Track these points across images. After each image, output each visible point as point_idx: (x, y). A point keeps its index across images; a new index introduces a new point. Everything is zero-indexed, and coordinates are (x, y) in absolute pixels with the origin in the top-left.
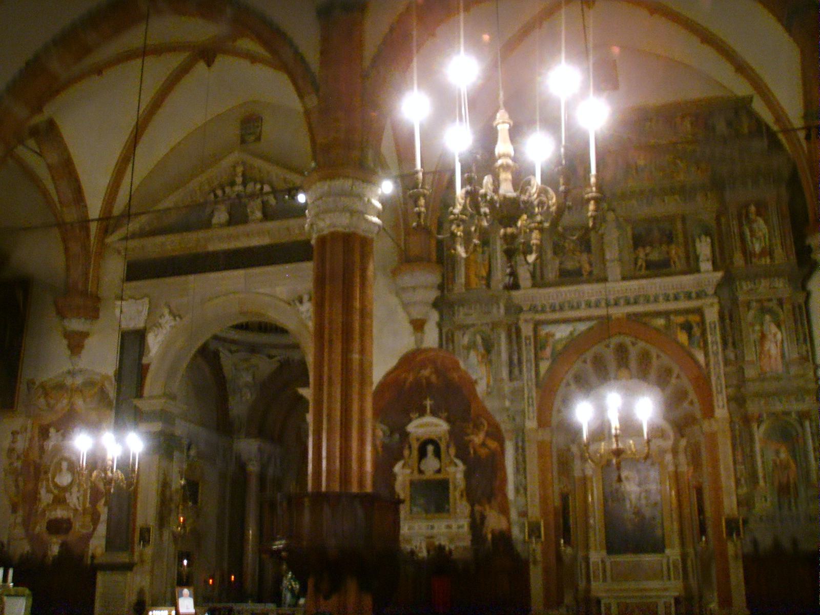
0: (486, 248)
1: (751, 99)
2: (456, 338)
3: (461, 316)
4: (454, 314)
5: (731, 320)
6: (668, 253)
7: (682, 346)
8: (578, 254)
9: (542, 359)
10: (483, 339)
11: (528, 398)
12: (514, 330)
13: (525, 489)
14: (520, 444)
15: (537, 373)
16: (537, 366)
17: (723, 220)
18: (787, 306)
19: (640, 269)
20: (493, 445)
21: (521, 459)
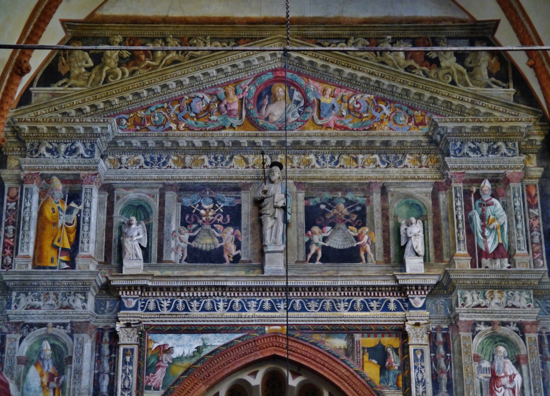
0: (73, 204)
1: (496, 24)
3: (21, 310)
5: (447, 348)
6: (357, 238)
8: (219, 227)
9: (148, 388)
10: (52, 346)
12: (106, 337)
17: (442, 197)
18: (532, 336)
19: (313, 260)
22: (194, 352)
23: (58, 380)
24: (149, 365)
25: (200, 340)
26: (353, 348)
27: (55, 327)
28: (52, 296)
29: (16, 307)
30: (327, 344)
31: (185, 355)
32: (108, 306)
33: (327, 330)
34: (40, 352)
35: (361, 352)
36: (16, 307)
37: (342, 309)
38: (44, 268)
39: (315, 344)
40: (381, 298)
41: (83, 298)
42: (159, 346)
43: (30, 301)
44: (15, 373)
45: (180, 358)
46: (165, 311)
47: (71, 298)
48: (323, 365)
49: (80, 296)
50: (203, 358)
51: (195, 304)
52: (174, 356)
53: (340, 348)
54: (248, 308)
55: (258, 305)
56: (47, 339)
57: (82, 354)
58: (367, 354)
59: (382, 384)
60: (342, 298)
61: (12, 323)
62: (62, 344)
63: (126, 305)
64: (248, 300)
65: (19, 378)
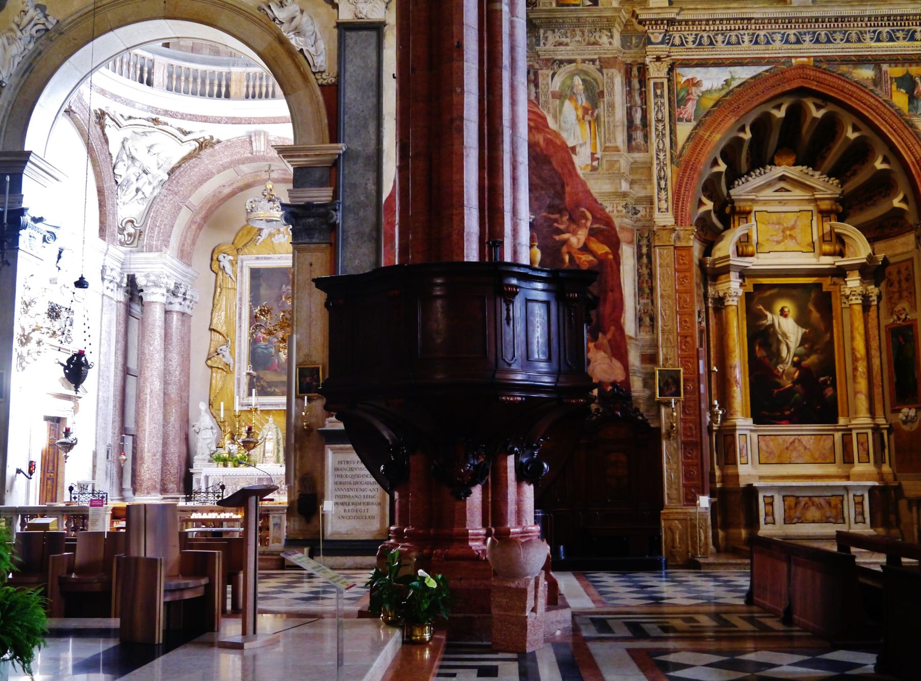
2: (540, 80)
3: (550, 46)
4: (538, 40)
7: (898, 113)
9: (681, 120)
10: (583, 80)
11: (660, 178)
12: (635, 71)
13: (653, 319)
14: (644, 250)
15: (673, 143)
16: (673, 132)
20: (601, 249)
21: (645, 271)
22: (722, 85)
23: (592, 113)
24: (680, 97)
25: (728, 73)
26: (881, 78)
27: (584, 63)
28: (578, 32)
29: (545, 44)
30: (854, 75)
31: (714, 88)
32: (634, 41)
33: (854, 61)
34: (572, 88)
35: (889, 82)
36: (545, 44)
37: (868, 40)
38: (568, 5)
39: (843, 75)
40: (906, 28)
41: (609, 34)
42: (688, 80)
43: (557, 38)
44: (551, 106)
45: (710, 91)
46: (691, 45)
47: (597, 35)
48: (851, 96)
49: (605, 32)
50: (732, 91)
51: (720, 38)
52: (703, 89)
53: (868, 79)
54: (774, 41)
55: (783, 37)
56: (577, 74)
57: (612, 89)
58: (895, 84)
59: (911, 113)
60: (867, 29)
61: (543, 60)
62: (593, 79)
63: (653, 40)
64: (773, 33)
65: (556, 111)
